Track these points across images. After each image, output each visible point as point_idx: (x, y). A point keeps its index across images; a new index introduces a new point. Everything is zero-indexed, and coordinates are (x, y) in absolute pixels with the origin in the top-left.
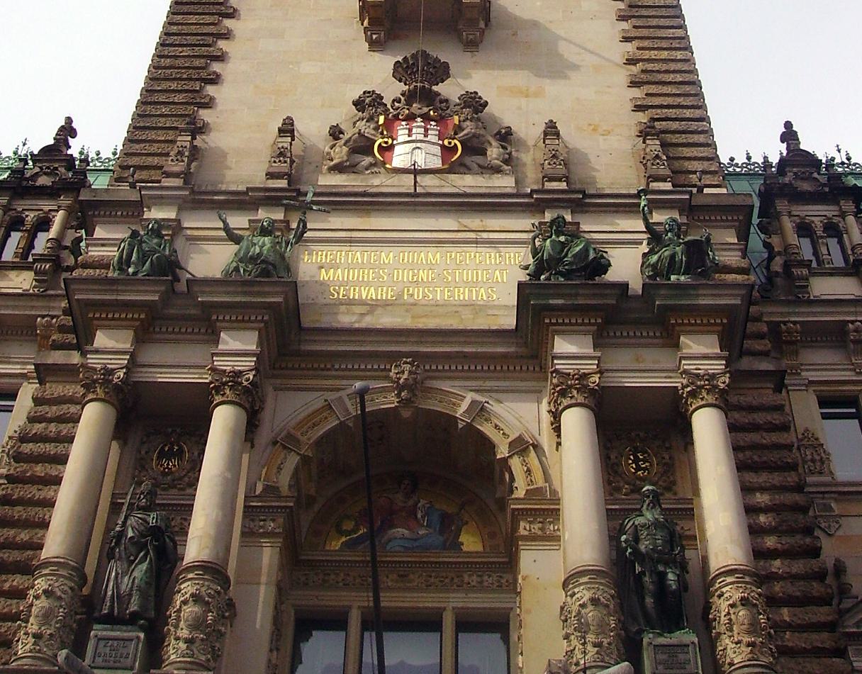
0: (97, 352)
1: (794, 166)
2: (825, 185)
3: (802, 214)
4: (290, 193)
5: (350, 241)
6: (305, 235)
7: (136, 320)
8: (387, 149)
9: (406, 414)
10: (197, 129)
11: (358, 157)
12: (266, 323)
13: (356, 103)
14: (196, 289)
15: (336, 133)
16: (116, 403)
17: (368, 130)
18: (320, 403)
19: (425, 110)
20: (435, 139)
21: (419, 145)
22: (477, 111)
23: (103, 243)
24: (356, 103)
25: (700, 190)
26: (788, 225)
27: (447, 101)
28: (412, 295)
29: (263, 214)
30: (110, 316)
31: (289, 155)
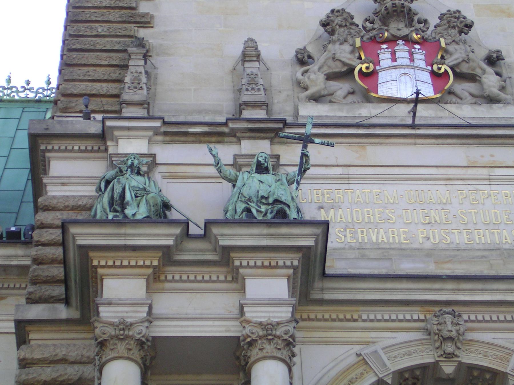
0: (110, 303)
4: (253, 123)
5: (347, 179)
6: (308, 172)
7: (148, 267)
8: (370, 76)
9: (448, 369)
11: (334, 85)
12: (295, 268)
13: (324, 24)
14: (215, 230)
15: (303, 59)
16: (140, 361)
17: (344, 52)
18: (353, 359)
19: (405, 31)
21: (406, 71)
23: (65, 181)
24: (324, 24)
27: (426, 21)
28: (428, 239)
29: (248, 146)
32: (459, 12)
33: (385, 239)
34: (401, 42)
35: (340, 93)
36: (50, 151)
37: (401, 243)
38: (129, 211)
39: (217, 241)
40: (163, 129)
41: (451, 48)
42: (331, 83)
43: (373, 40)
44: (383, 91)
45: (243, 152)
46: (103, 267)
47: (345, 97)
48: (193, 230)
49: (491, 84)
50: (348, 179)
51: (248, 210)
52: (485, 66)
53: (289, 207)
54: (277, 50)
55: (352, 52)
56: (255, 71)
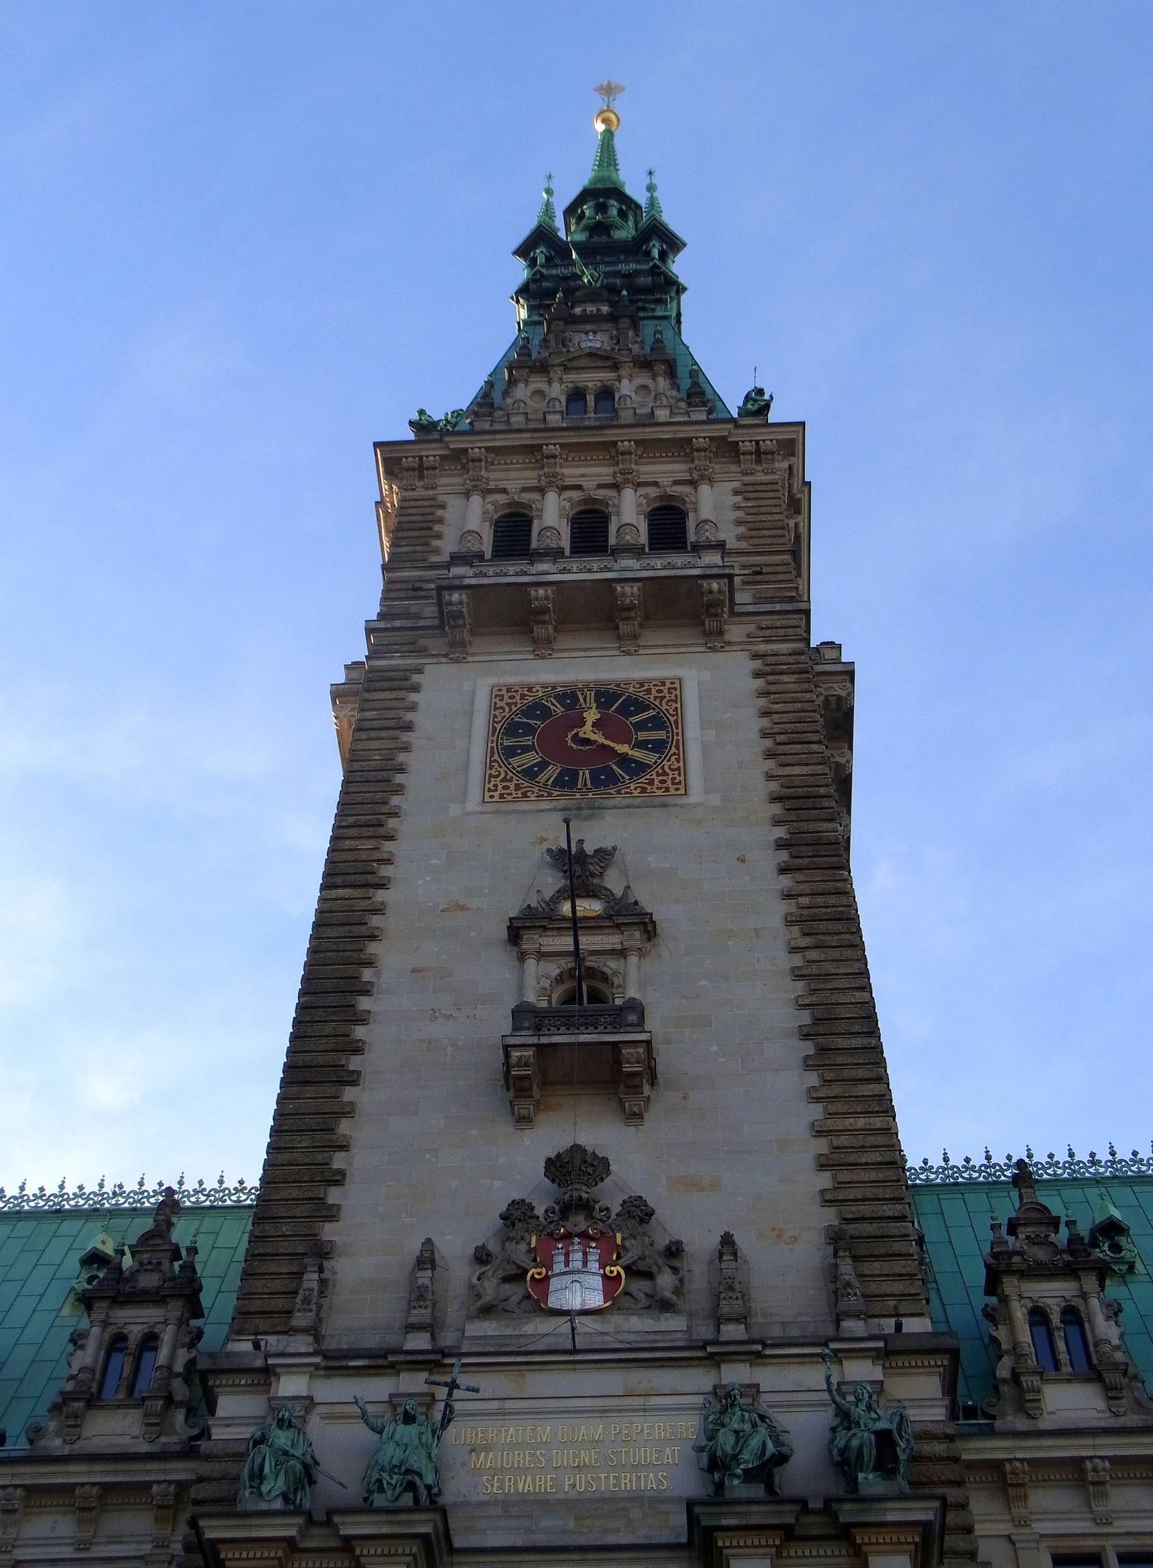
1: (1025, 1224)
2: (1063, 1251)
3: (1035, 1296)
5: (502, 1413)
10: (322, 1253)
12: (414, 1556)
14: (337, 1519)
15: (482, 1257)
17: (519, 1252)
20: (594, 1266)
22: (642, 1221)
23: (229, 1422)
25: (899, 1327)
26: (1019, 1313)
27: (607, 1209)
30: (244, 1555)
31: (430, 1296)
32: (641, 1198)
33: (531, 1489)
34: (577, 1240)
35: (515, 1299)
36: (218, 1386)
37: (546, 1492)
38: (265, 1489)
39: (338, 1530)
40: (323, 1364)
41: (628, 1244)
42: (507, 1286)
43: (551, 1235)
44: (553, 1302)
45: (402, 1390)
46: (230, 1560)
47: (519, 1303)
48: (316, 1518)
49: (664, 1286)
50: (505, 1414)
51: (380, 1481)
52: (660, 1261)
53: (420, 1475)
54: (455, 1247)
55: (530, 1251)
56: (427, 1282)
